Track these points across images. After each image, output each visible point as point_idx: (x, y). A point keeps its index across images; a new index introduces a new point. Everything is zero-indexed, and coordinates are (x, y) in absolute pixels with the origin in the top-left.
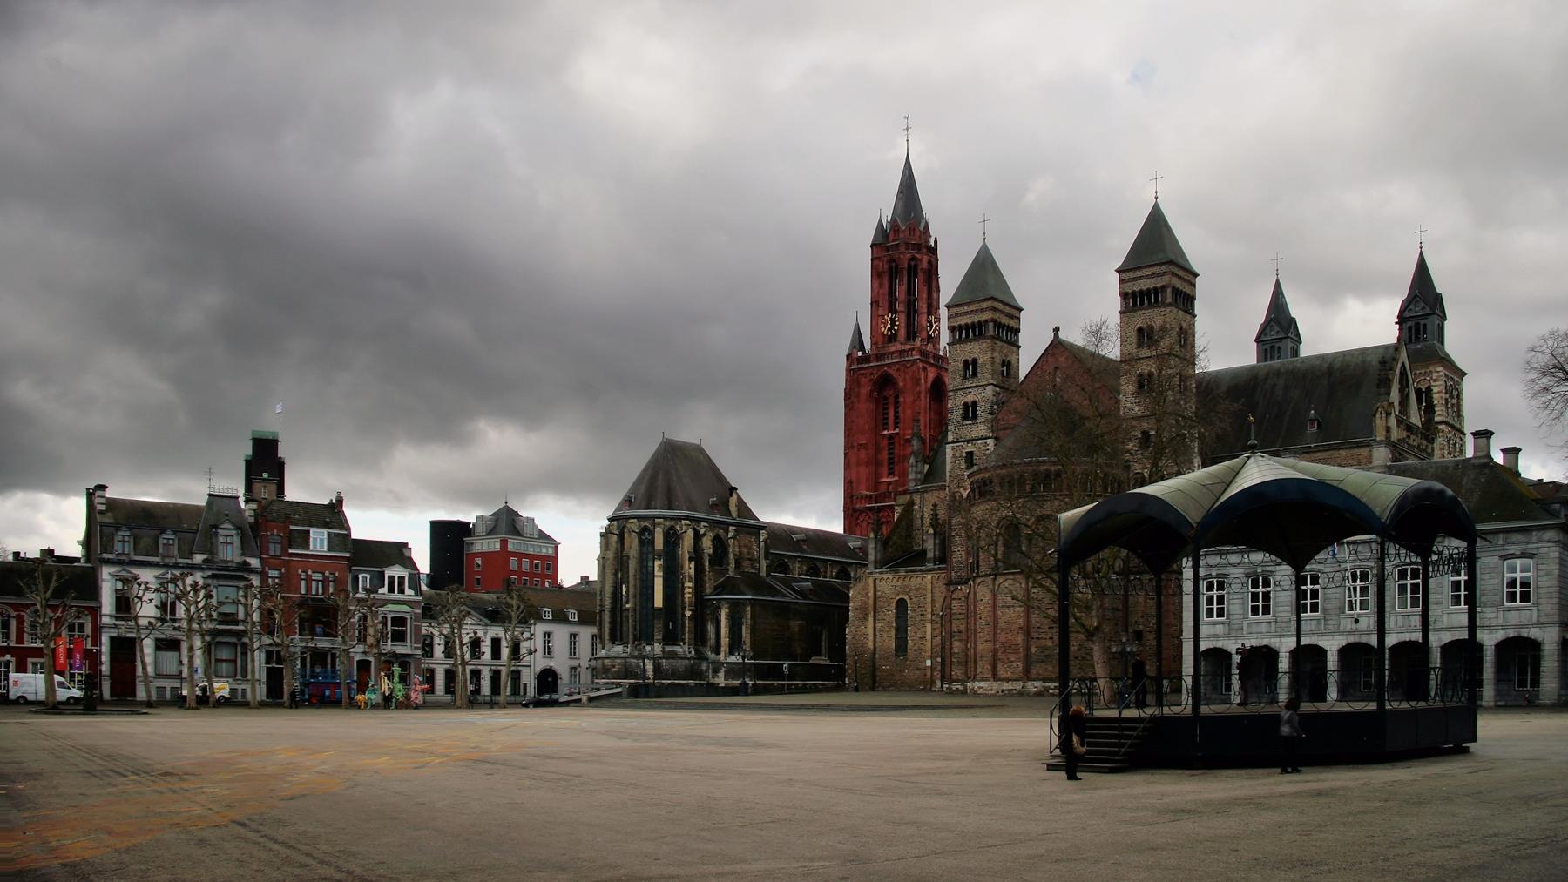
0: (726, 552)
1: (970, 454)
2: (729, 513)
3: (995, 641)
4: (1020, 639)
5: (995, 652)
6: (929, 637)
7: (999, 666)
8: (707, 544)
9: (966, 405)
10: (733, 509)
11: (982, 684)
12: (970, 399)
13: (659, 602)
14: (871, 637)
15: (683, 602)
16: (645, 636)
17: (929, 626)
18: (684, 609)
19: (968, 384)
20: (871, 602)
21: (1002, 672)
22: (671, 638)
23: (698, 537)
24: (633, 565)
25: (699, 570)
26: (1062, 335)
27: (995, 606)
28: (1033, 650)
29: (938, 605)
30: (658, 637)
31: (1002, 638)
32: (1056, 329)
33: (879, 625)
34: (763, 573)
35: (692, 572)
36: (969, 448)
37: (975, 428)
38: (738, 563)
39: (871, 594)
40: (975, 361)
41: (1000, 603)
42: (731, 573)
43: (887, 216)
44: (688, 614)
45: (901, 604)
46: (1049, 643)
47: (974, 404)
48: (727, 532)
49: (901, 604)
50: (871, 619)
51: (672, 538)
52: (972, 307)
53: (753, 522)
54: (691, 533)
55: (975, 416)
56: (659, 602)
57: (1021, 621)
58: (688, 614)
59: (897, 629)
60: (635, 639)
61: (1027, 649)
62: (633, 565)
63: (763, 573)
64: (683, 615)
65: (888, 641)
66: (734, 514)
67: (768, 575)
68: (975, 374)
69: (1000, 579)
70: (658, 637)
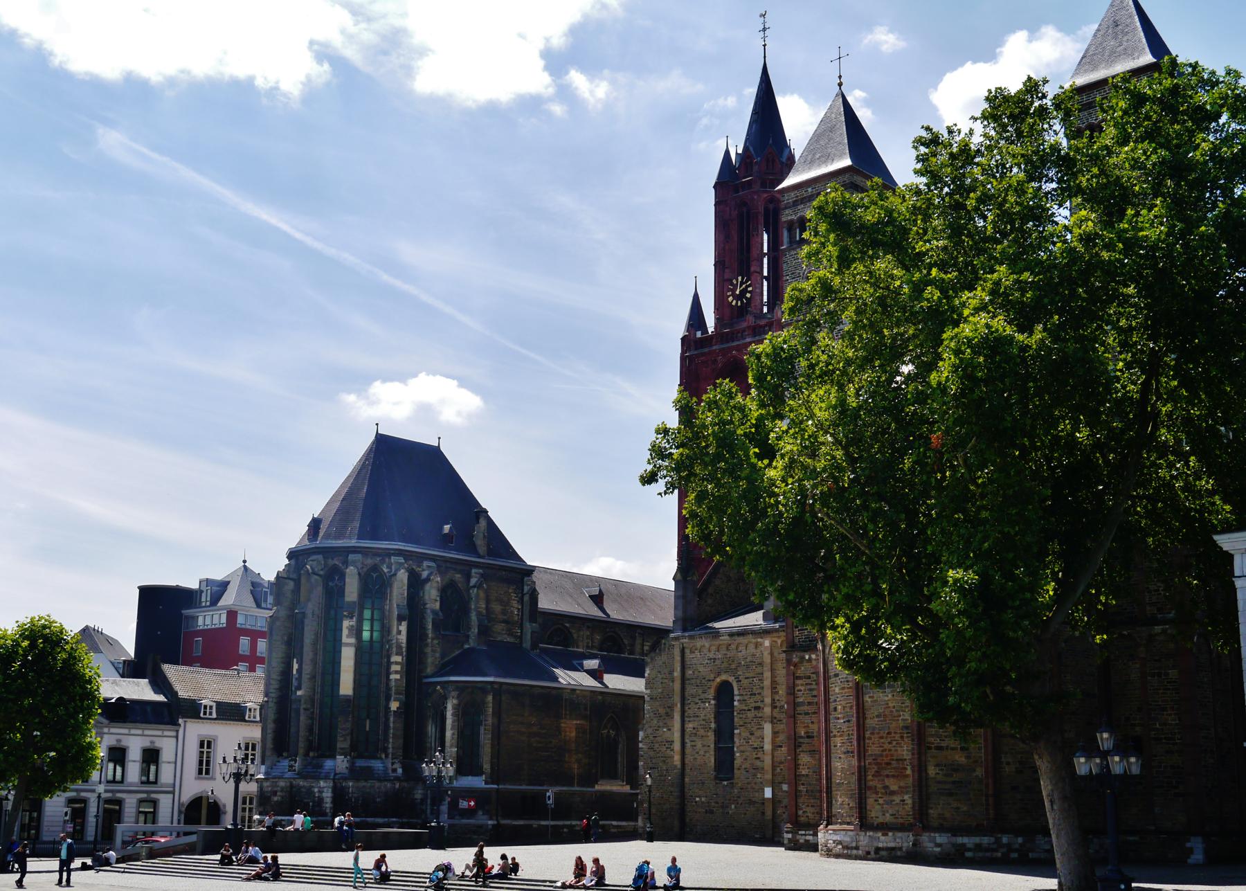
0: (465, 610)
2: (473, 549)
4: (905, 750)
6: (768, 747)
8: (432, 595)
10: (480, 543)
13: (346, 686)
14: (677, 746)
15: (388, 688)
16: (323, 747)
17: (768, 728)
18: (388, 699)
20: (677, 686)
21: (876, 812)
22: (363, 747)
23: (416, 583)
24: (310, 630)
25: (415, 635)
28: (932, 771)
30: (343, 744)
31: (873, 749)
33: (689, 726)
34: (527, 644)
35: (403, 638)
38: (484, 631)
39: (677, 674)
42: (472, 643)
43: (737, 147)
44: (394, 706)
45: (724, 692)
46: (960, 758)
48: (468, 577)
49: (724, 692)
50: (677, 717)
51: (375, 586)
53: (511, 563)
54: (403, 576)
56: (346, 686)
58: (394, 706)
59: (719, 733)
60: (310, 748)
61: (921, 769)
62: (310, 630)
63: (527, 644)
64: (387, 708)
65: (704, 753)
66: (482, 549)
67: (534, 646)
70: (343, 744)
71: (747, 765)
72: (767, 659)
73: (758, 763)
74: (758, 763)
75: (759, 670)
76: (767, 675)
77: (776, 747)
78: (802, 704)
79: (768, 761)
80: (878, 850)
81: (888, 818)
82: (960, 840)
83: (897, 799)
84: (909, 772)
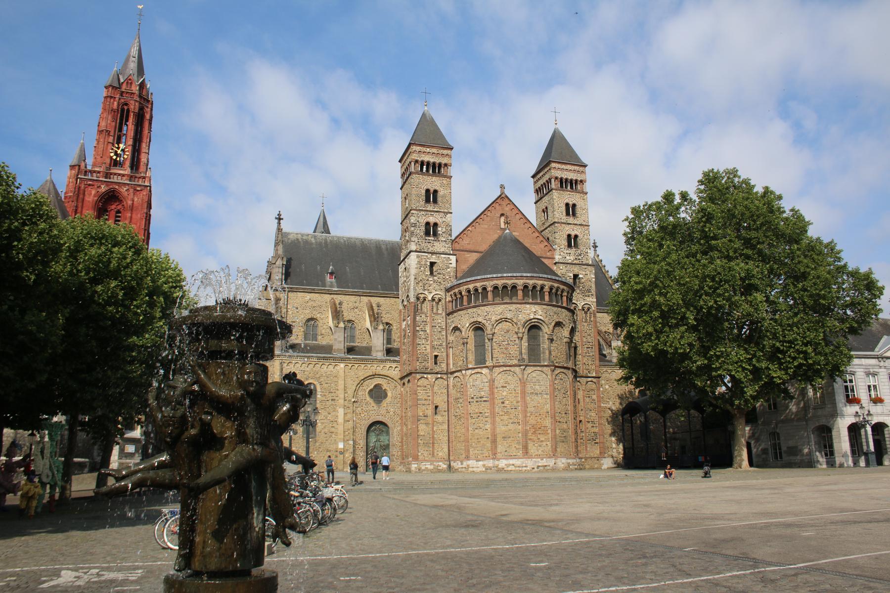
1: (432, 264)
3: (526, 423)
4: (548, 422)
5: (525, 434)
6: (341, 419)
7: (530, 445)
9: (428, 224)
11: (511, 462)
12: (432, 220)
17: (341, 411)
19: (430, 207)
26: (507, 192)
27: (524, 393)
28: (558, 432)
29: (350, 392)
32: (502, 187)
36: (433, 259)
37: (436, 244)
40: (435, 192)
41: (529, 389)
46: (565, 426)
47: (436, 225)
52: (434, 150)
55: (435, 234)
57: (548, 406)
68: (435, 201)
69: (529, 370)
71: (326, 430)
72: (342, 373)
73: (333, 430)
74: (333, 430)
75: (335, 379)
76: (341, 383)
77: (346, 421)
78: (421, 400)
79: (340, 429)
80: (538, 467)
81: (540, 452)
82: (569, 461)
83: (544, 444)
84: (549, 431)
